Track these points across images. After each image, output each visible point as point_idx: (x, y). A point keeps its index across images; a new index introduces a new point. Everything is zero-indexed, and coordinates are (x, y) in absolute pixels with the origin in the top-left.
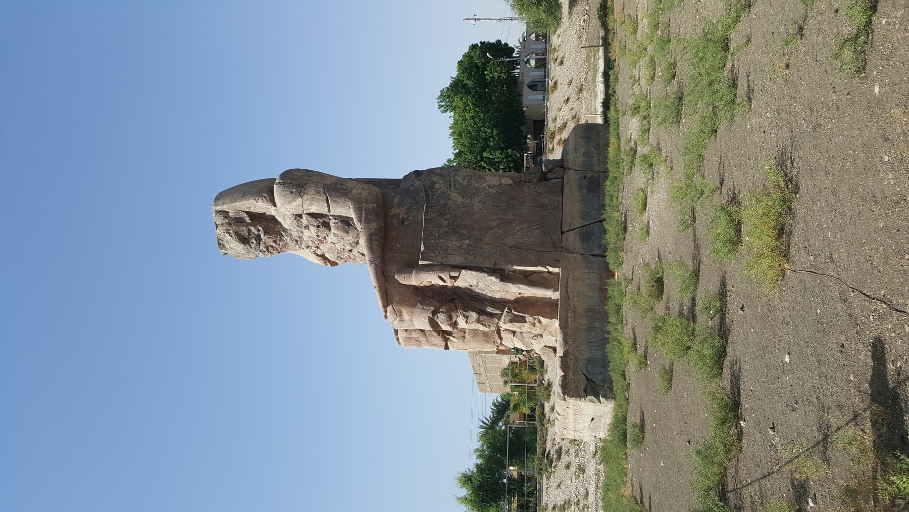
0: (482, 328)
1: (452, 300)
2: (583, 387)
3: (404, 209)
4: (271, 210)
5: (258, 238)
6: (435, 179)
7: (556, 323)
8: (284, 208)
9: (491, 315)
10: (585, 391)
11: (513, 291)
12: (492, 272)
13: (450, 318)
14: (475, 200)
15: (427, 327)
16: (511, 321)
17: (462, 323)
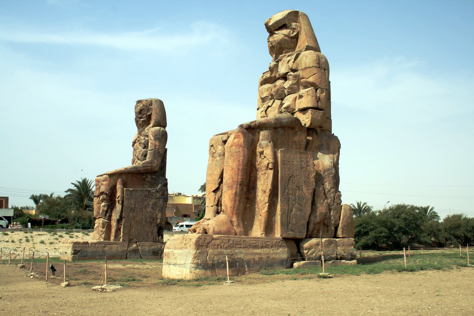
0: (101, 211)
1: (111, 200)
2: (77, 249)
3: (150, 180)
4: (151, 125)
5: (141, 118)
6: (160, 193)
7: (102, 240)
8: (151, 130)
9: (106, 215)
10: (75, 250)
11: (114, 224)
12: (121, 217)
13: (104, 200)
14: (151, 209)
15: (101, 191)
16: (103, 223)
17: (103, 204)
